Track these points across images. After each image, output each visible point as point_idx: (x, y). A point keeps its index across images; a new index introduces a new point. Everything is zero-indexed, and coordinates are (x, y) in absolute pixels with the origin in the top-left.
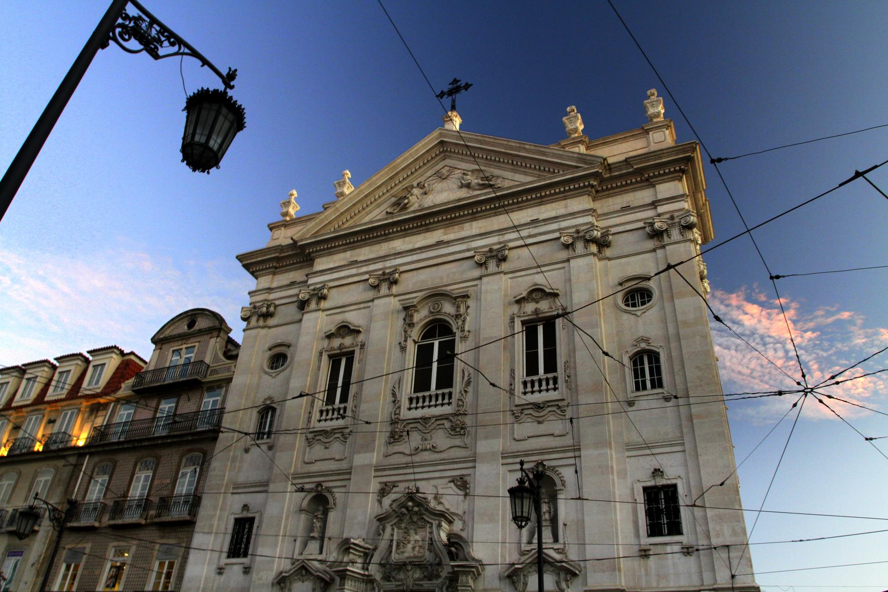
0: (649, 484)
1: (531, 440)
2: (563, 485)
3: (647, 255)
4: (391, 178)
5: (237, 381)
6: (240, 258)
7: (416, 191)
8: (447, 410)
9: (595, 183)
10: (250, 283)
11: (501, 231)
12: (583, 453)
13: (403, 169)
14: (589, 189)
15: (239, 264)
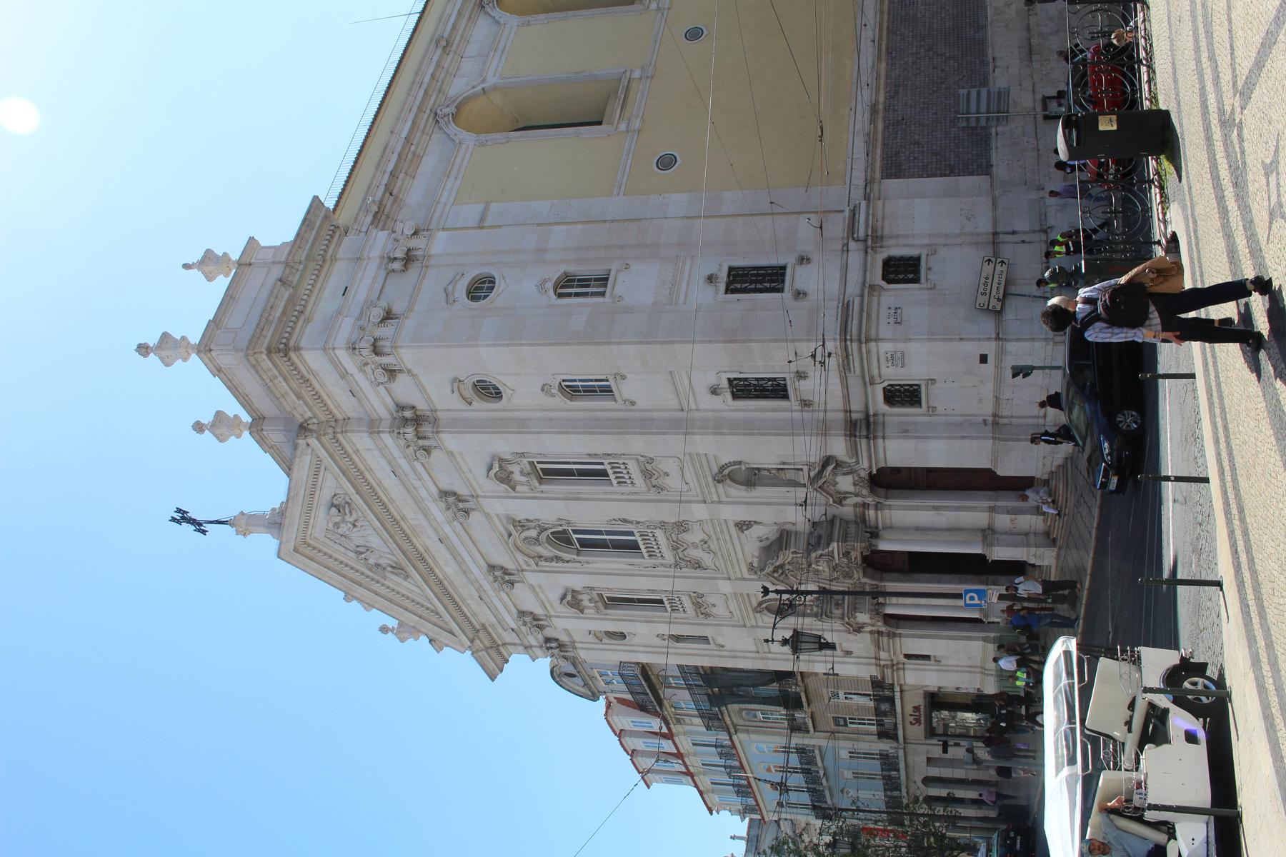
0: (729, 396)
1: (689, 479)
2: (740, 463)
3: (423, 380)
4: (360, 585)
5: (644, 659)
6: (493, 678)
7: (372, 561)
8: (658, 533)
9: (330, 431)
10: (518, 661)
11: (418, 501)
12: (701, 451)
13: (344, 577)
14: (339, 436)
15: (500, 676)
